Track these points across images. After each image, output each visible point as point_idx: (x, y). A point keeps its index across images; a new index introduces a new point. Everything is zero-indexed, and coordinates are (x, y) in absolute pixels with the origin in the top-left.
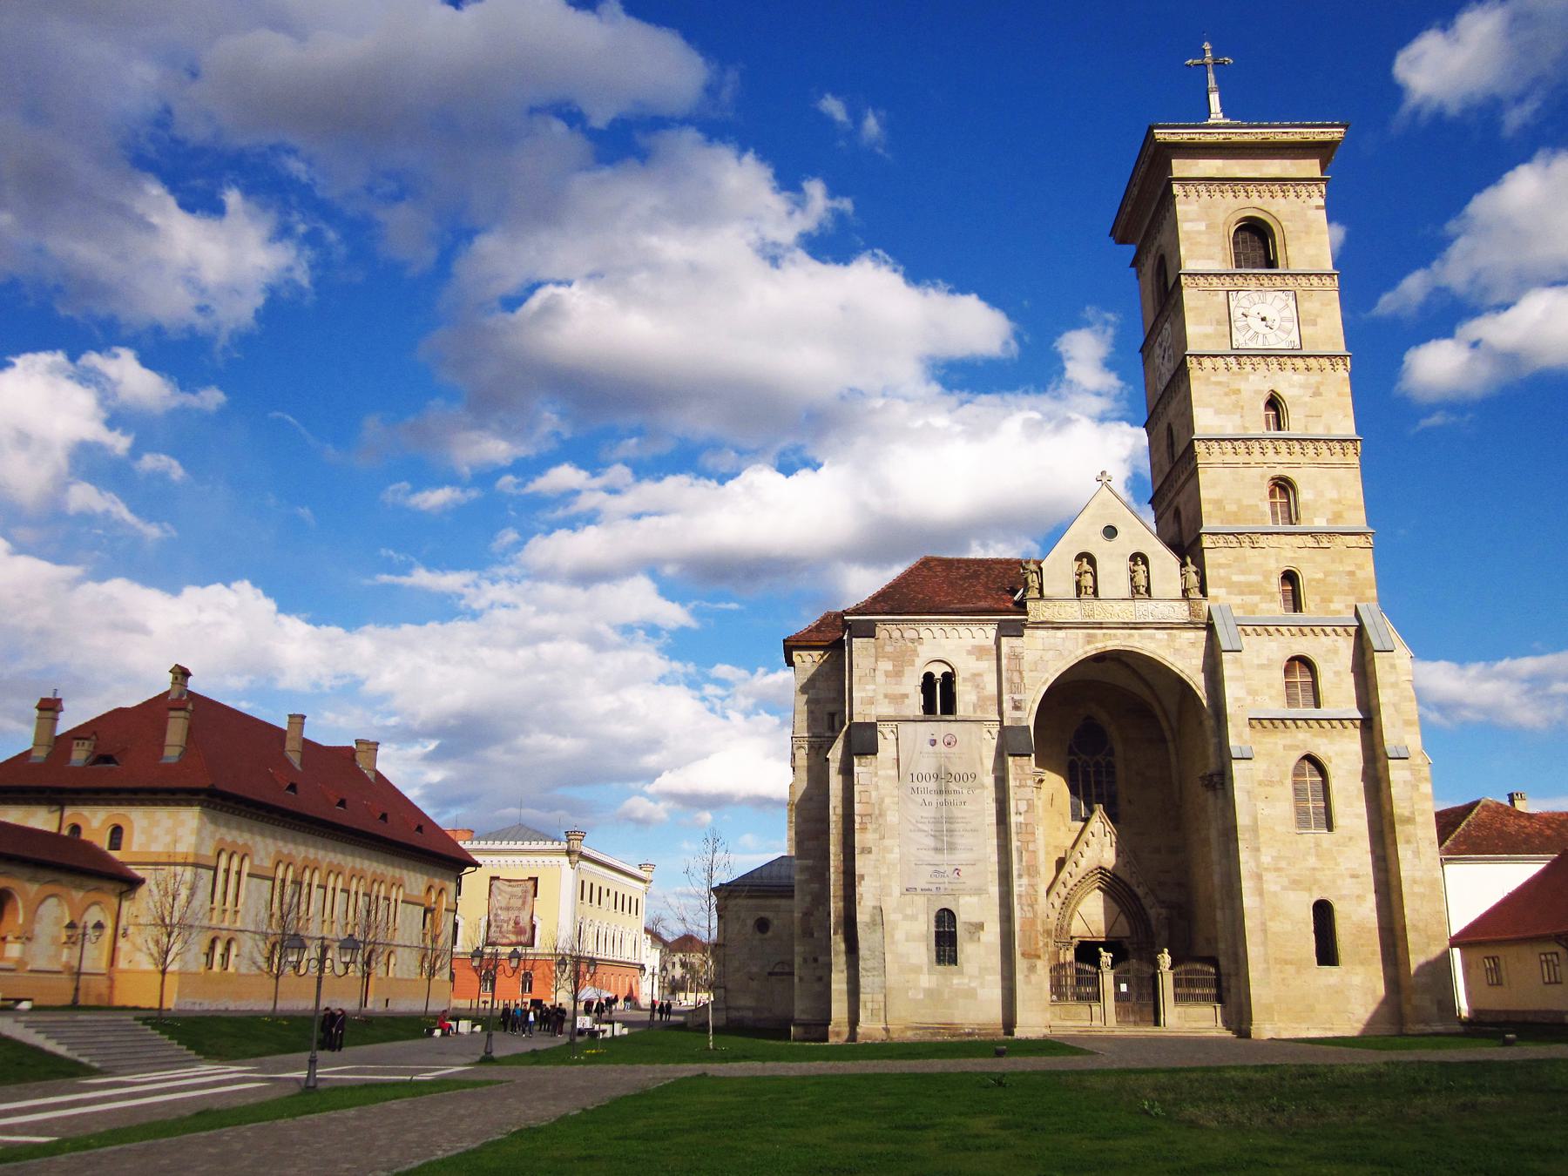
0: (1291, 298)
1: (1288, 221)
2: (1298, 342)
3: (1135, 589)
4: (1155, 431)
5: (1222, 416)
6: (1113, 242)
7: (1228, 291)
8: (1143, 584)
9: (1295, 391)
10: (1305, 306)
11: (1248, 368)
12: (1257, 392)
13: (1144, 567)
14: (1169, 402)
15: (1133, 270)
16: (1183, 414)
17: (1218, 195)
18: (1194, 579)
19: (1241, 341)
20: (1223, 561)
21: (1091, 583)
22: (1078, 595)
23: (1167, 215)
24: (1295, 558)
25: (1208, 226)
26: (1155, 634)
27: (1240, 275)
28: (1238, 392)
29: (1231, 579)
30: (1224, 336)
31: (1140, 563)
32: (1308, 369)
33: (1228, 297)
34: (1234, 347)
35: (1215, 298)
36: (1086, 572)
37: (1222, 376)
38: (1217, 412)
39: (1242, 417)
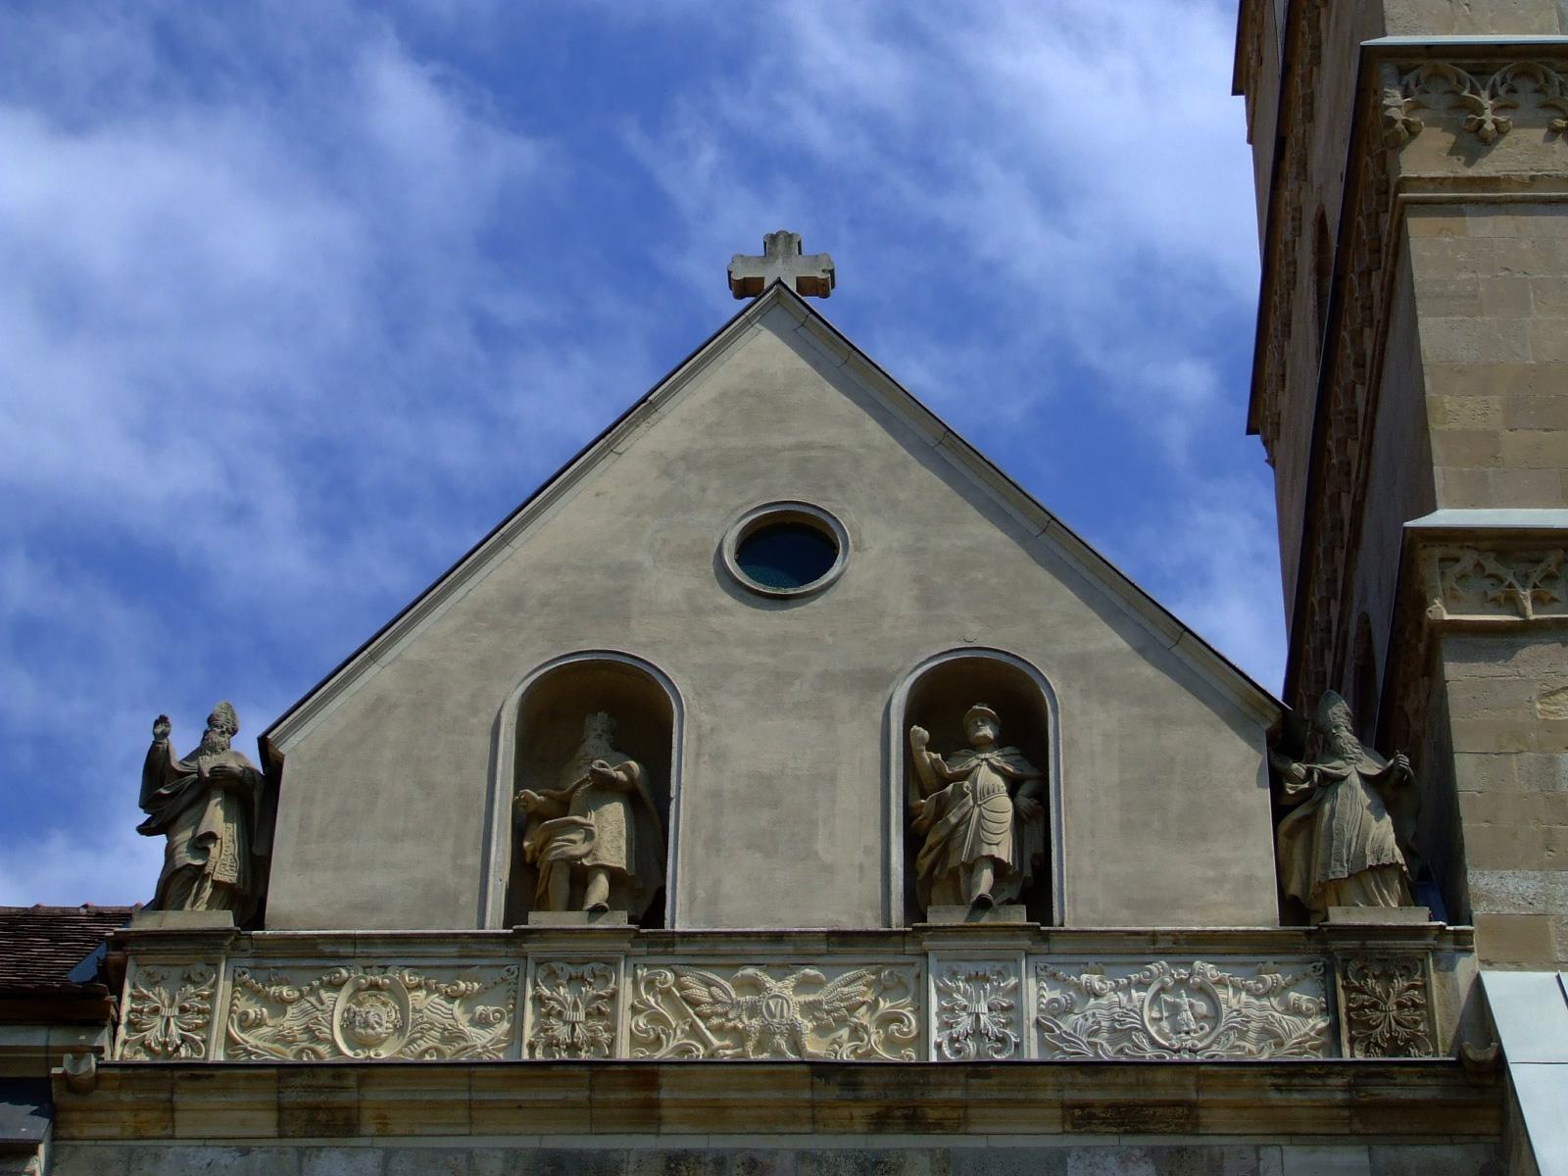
8: (1004, 851)
26: (1062, 1156)
36: (604, 788)
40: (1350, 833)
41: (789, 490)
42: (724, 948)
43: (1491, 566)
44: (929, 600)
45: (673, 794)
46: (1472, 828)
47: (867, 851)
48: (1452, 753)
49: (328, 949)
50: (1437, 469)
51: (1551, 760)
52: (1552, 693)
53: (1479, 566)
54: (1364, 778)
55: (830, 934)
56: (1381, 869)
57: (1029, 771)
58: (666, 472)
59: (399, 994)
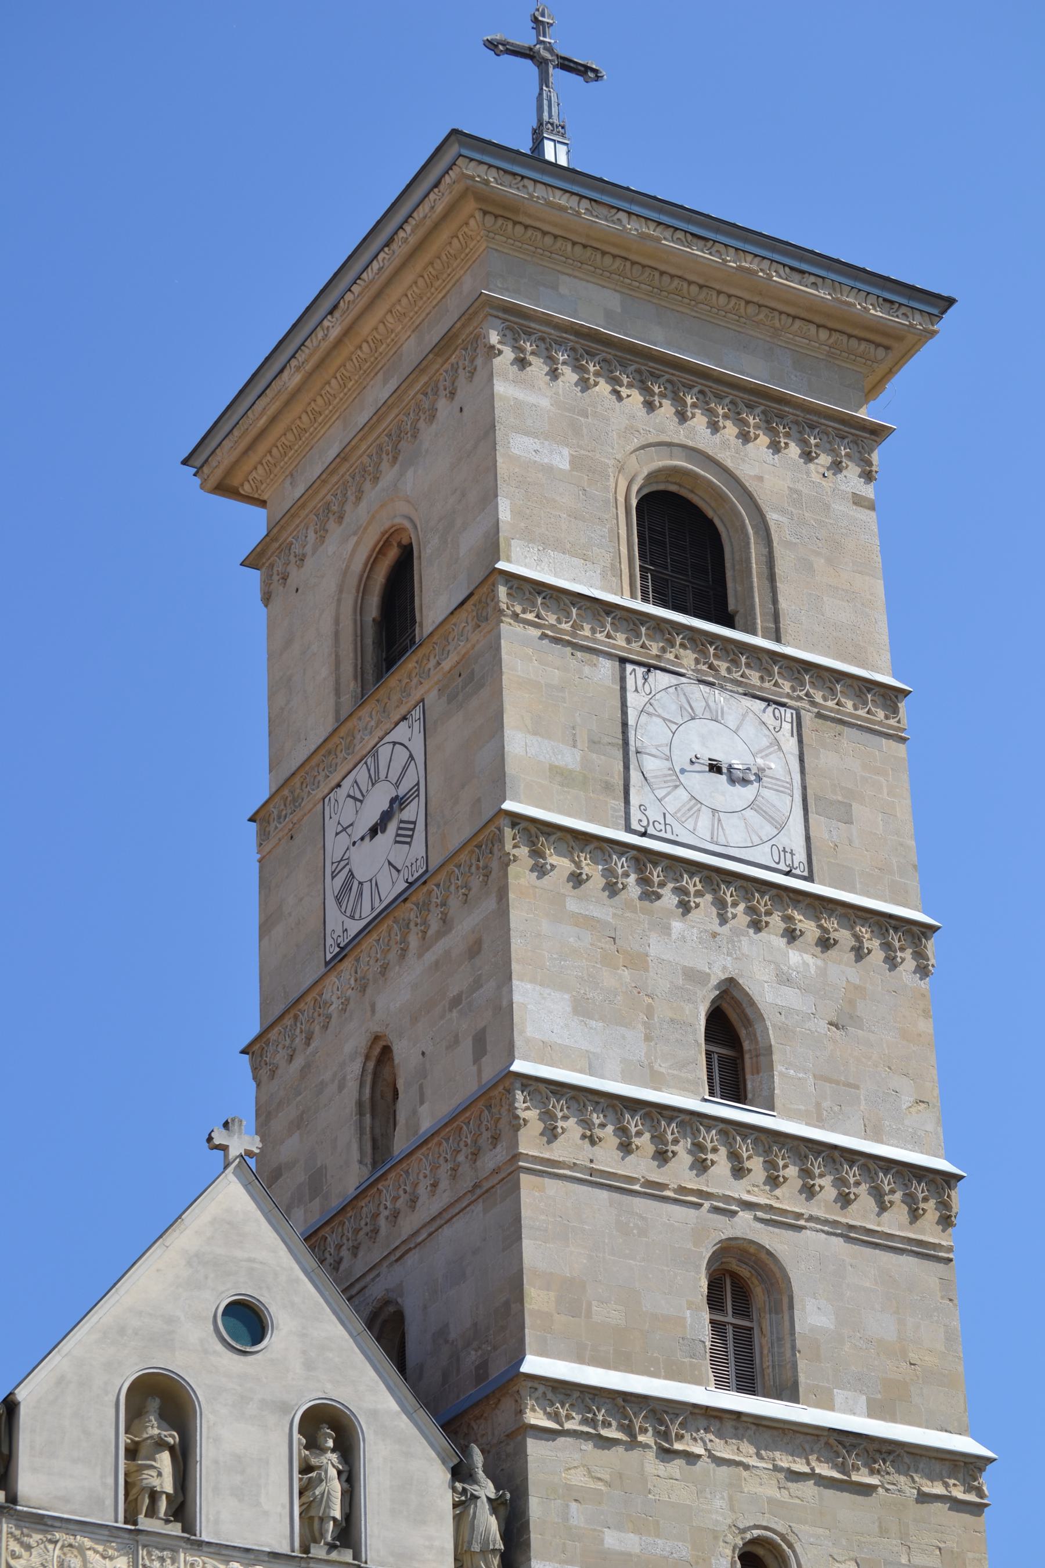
0: (787, 726)
1: (783, 511)
2: (801, 856)
3: (310, 1536)
4: (299, 1061)
5: (593, 1023)
6: (197, 481)
7: (623, 661)
9: (791, 998)
10: (823, 760)
11: (669, 899)
12: (694, 976)
13: (334, 1457)
14: (384, 969)
15: (255, 576)
16: (456, 1001)
17: (603, 388)
18: (489, 1524)
19: (654, 814)
20: (578, 1478)
21: (167, 1484)
22: (131, 1517)
23: (442, 404)
24: (782, 1504)
25: (574, 461)
27: (659, 626)
28: (638, 961)
29: (602, 1541)
30: (608, 787)
31: (330, 1443)
32: (825, 943)
33: (623, 679)
34: (635, 825)
35: (587, 670)
36: (161, 1444)
37: (603, 910)
38: (582, 1009)
39: (648, 1038)
40: (482, 1529)
41: (247, 1289)
42: (224, 1552)
43: (550, 1395)
44: (309, 1365)
45: (198, 1459)
46: (536, 1538)
47: (283, 1506)
48: (528, 1495)
49: (50, 1522)
50: (527, 1331)
51: (567, 1506)
52: (570, 1469)
53: (544, 1393)
54: (488, 1498)
55: (269, 1553)
56: (494, 1550)
57: (347, 1468)
58: (189, 1263)
59: (81, 1550)
